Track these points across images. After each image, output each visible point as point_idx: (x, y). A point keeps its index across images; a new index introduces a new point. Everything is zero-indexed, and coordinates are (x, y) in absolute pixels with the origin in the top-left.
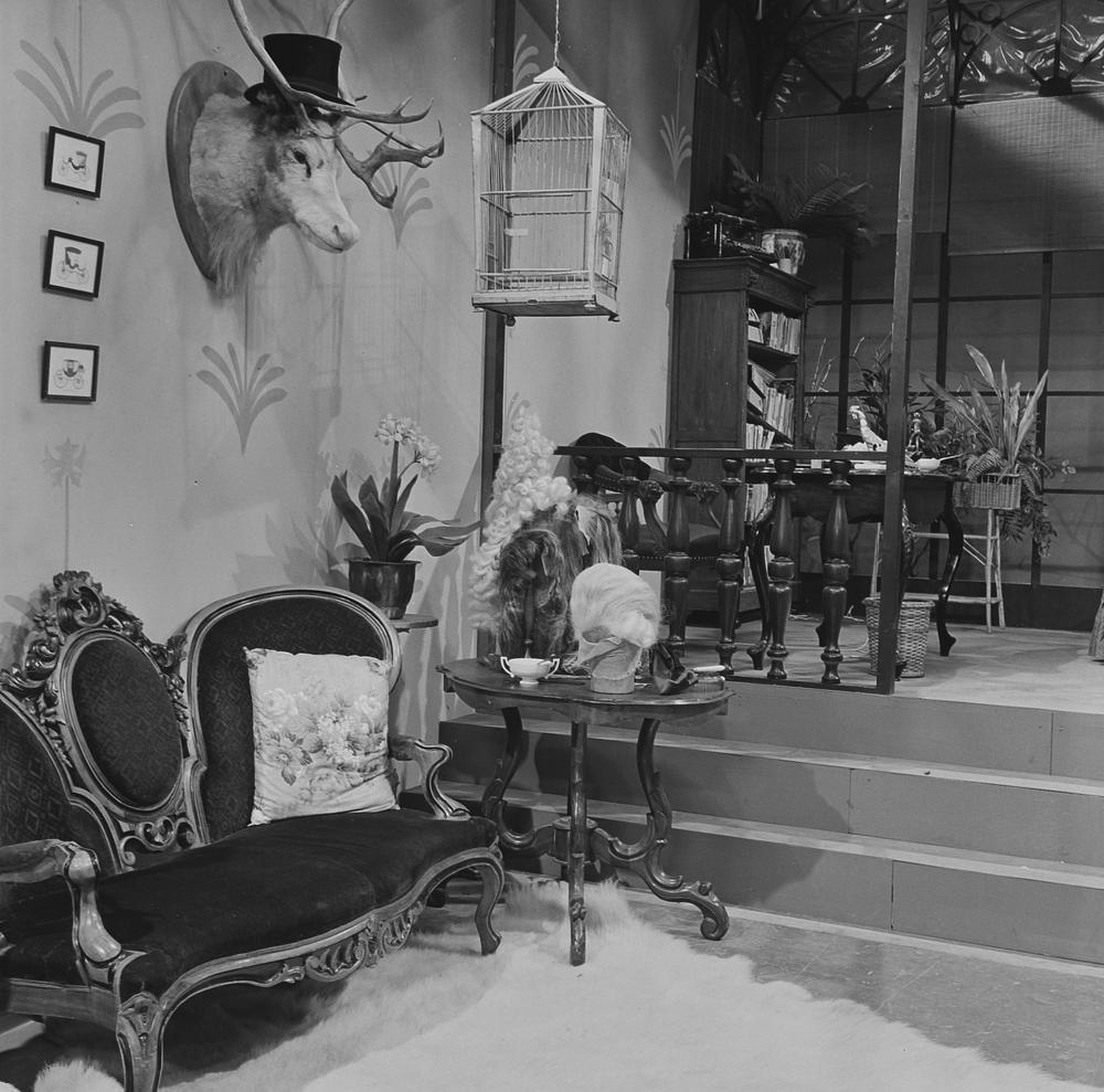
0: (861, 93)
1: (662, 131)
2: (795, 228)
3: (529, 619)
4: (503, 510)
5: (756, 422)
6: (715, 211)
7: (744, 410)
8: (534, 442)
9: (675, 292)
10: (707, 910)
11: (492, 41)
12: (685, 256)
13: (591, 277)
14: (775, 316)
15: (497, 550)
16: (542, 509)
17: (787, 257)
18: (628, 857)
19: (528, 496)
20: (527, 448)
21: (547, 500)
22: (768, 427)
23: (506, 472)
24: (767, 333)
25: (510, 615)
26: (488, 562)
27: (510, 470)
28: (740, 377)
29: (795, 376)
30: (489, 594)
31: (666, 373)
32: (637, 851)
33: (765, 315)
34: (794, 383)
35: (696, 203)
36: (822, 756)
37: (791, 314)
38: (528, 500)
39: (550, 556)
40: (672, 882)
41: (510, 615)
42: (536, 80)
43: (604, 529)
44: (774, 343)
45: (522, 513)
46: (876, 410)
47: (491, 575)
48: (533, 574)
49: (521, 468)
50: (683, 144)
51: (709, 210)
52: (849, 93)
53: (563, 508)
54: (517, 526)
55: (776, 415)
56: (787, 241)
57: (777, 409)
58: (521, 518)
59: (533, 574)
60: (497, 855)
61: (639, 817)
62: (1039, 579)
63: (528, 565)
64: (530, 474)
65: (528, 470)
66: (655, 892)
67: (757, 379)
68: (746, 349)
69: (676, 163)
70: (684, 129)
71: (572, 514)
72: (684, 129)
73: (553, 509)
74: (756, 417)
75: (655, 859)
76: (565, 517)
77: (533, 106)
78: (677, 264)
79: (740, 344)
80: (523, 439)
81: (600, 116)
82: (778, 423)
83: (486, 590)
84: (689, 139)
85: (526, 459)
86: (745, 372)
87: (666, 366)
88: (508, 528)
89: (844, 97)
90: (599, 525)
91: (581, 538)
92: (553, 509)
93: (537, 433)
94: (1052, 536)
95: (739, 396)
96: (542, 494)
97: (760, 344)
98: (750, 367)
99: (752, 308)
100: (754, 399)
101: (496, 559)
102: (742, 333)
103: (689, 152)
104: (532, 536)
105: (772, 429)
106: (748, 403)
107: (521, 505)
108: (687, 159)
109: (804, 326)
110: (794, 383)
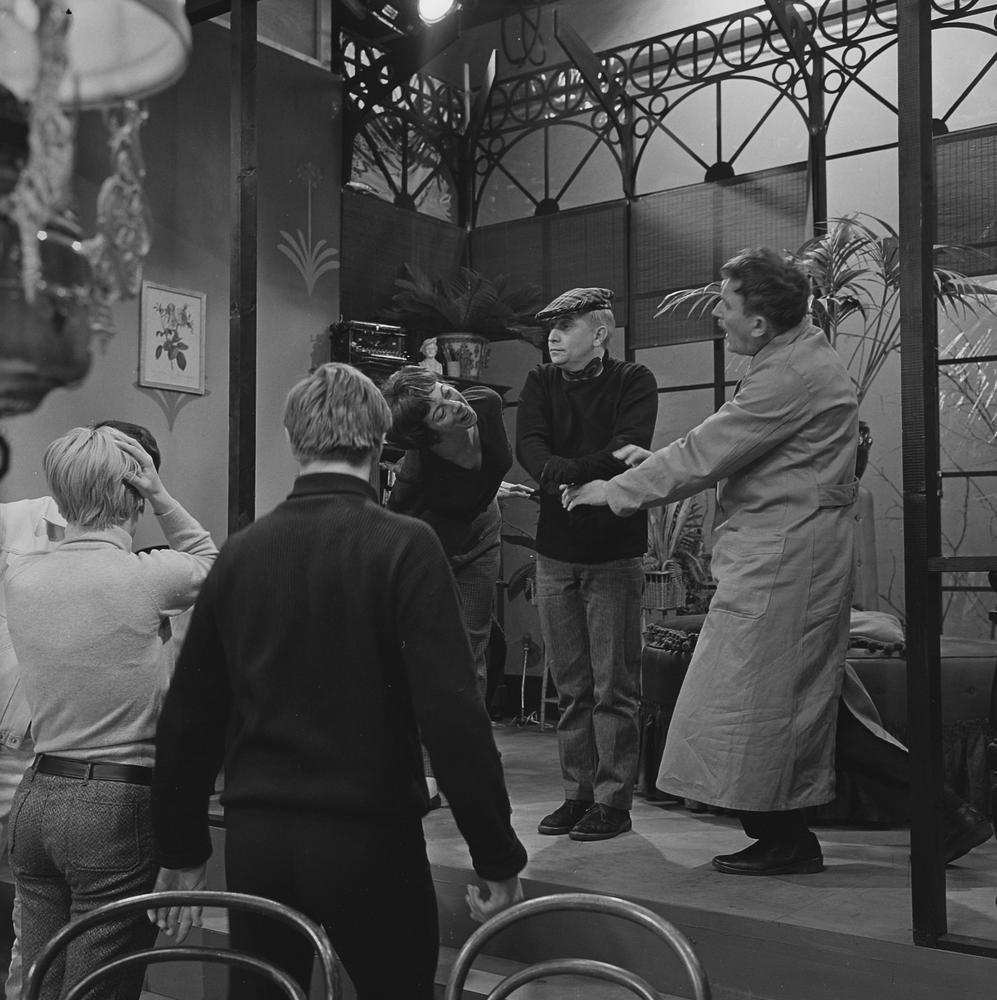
0: (553, 195)
1: (281, 247)
2: (466, 331)
17: (454, 359)
52: (543, 198)
56: (460, 344)
69: (311, 274)
84: (334, 251)
89: (539, 200)
103: (336, 265)
108: (328, 273)
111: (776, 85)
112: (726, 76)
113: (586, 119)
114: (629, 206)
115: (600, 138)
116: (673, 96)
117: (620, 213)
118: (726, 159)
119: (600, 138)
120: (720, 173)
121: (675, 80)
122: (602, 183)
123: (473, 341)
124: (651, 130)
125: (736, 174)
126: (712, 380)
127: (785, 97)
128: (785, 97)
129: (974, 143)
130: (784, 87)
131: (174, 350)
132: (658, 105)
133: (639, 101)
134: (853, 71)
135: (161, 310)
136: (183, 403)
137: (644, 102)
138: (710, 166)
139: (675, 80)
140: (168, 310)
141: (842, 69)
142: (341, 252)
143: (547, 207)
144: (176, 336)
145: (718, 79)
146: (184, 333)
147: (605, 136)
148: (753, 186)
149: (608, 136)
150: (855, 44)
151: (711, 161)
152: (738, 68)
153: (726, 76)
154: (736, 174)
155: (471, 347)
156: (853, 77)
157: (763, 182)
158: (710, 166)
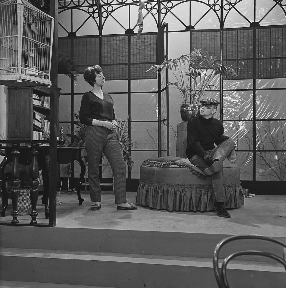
5: (39, 131)
7: (32, 128)
9: (8, 88)
14: (46, 98)
24: (43, 103)
28: (30, 117)
36: (32, 252)
46: (80, 127)
62: (130, 177)
68: (32, 108)
74: (37, 129)
79: (30, 105)
86: (32, 115)
94: (133, 164)
98: (34, 114)
100: (37, 123)
102: (30, 102)
112: (131, 4)
113: (86, 9)
115: (91, 15)
116: (115, 7)
118: (132, 28)
119: (91, 15)
124: (107, 16)
125: (134, 33)
126: (70, 93)
130: (149, 10)
132: (110, 9)
133: (104, 6)
134: (169, 9)
137: (106, 7)
138: (127, 29)
141: (166, 8)
143: (72, 35)
145: (72, 8)
147: (92, 15)
149: (93, 15)
151: (127, 28)
153: (131, 4)
154: (134, 33)
156: (169, 11)
158: (127, 29)
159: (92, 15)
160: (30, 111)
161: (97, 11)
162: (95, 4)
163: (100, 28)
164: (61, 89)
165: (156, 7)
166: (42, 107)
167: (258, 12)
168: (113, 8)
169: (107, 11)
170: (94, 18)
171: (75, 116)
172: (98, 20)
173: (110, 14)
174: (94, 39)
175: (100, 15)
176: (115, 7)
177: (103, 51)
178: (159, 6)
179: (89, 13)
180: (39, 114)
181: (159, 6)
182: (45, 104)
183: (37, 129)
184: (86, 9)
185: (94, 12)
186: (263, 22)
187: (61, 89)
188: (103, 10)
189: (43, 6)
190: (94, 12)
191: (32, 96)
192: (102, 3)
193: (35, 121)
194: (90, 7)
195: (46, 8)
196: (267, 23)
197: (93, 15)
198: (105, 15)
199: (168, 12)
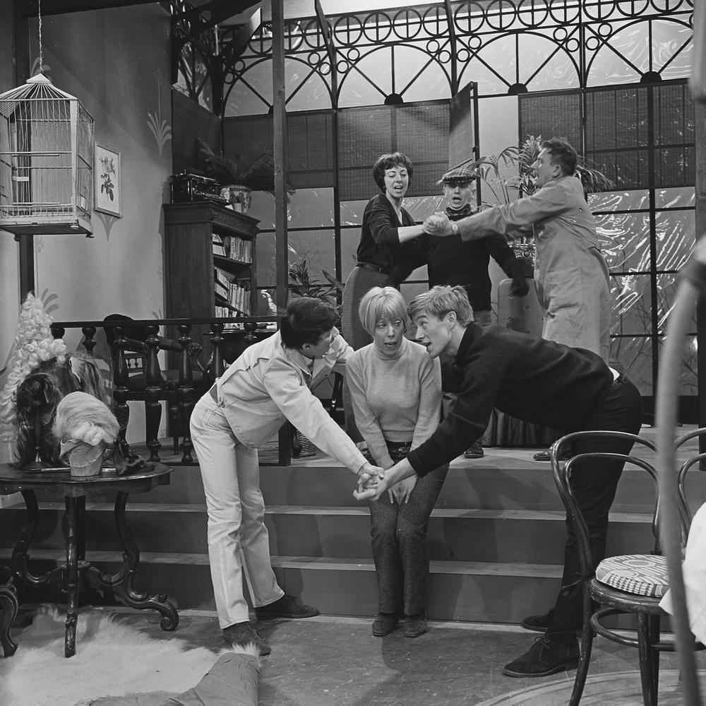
1: (149, 123)
2: (243, 185)
3: (38, 433)
4: (18, 362)
5: (224, 306)
6: (188, 173)
7: (213, 298)
8: (38, 317)
10: (163, 612)
11: (14, 60)
12: (171, 202)
13: (75, 209)
14: (233, 240)
15: (14, 389)
16: (44, 360)
17: (238, 202)
18: (111, 584)
19: (34, 352)
20: (33, 321)
21: (48, 354)
22: (231, 309)
23: (19, 337)
24: (228, 250)
25: (24, 430)
26: (8, 397)
27: (22, 336)
28: (209, 277)
29: (250, 276)
30: (10, 418)
31: (162, 276)
32: (118, 578)
33: (227, 239)
34: (250, 281)
35: (176, 168)
37: (244, 238)
38: (35, 355)
39: (50, 390)
40: (139, 596)
41: (24, 430)
42: (28, 81)
43: (90, 371)
44: (234, 256)
45: (31, 363)
47: (10, 405)
48: (38, 403)
49: (29, 334)
50: (165, 131)
51: (183, 172)
53: (61, 359)
54: (28, 372)
55: (238, 301)
57: (238, 297)
58: (30, 366)
59: (38, 403)
60: (12, 590)
61: (118, 558)
63: (35, 398)
64: (36, 338)
65: (35, 335)
66: (131, 605)
67: (221, 278)
68: (212, 261)
69: (161, 143)
70: (165, 122)
71: (68, 363)
72: (165, 122)
73: (54, 360)
74: (222, 302)
75: (130, 583)
76: (64, 365)
77: (28, 97)
78: (165, 207)
79: (208, 256)
80: (30, 315)
81: (74, 107)
82: (239, 306)
83: (9, 416)
84: (169, 128)
85: (33, 328)
86: (212, 274)
87: (161, 271)
88: (22, 374)
90: (86, 369)
91: (75, 379)
92: (54, 360)
93: (40, 311)
95: (210, 289)
96: (44, 350)
97: (224, 256)
98: (215, 272)
99: (216, 234)
100: (220, 291)
101: (14, 394)
102: (209, 249)
103: (169, 137)
104: (36, 378)
105: (235, 310)
106: (216, 292)
107: (31, 358)
108: (167, 141)
109: (254, 245)
110: (250, 281)
111: (429, 53)
113: (304, 57)
114: (336, 114)
115: (314, 70)
117: (330, 117)
118: (398, 92)
119: (314, 70)
120: (394, 100)
121: (363, 40)
122: (314, 97)
123: (246, 191)
124: (349, 70)
125: (404, 102)
127: (356, 65)
128: (356, 65)
129: (561, 98)
130: (433, 54)
131: (108, 186)
134: (475, 51)
135: (102, 161)
136: (112, 223)
137: (345, 51)
139: (363, 40)
140: (106, 161)
142: (172, 127)
144: (109, 180)
146: (111, 175)
147: (318, 69)
148: (417, 110)
149: (319, 69)
150: (476, 36)
151: (389, 93)
152: (405, 40)
153: (397, 43)
154: (404, 102)
155: (245, 194)
156: (475, 54)
157: (422, 108)
159: (318, 69)
160: (208, 266)
161: (327, 60)
162: (324, 46)
163: (335, 94)
164: (259, 221)
165: (448, 47)
166: (228, 259)
167: (657, 49)
168: (359, 53)
169: (348, 60)
170: (320, 74)
171: (290, 274)
172: (328, 78)
173: (353, 66)
174: (322, 118)
175: (334, 69)
176: (363, 51)
177: (340, 140)
178: (453, 47)
179: (310, 65)
180: (224, 272)
181: (453, 47)
182: (232, 253)
183: (222, 302)
184: (304, 57)
185: (320, 63)
186: (667, 71)
187: (259, 221)
188: (339, 58)
189: (217, 54)
190: (320, 63)
191: (211, 238)
192: (337, 44)
193: (218, 286)
194: (313, 52)
195: (224, 57)
196: (674, 75)
197: (319, 69)
198: (343, 67)
199: (472, 56)
